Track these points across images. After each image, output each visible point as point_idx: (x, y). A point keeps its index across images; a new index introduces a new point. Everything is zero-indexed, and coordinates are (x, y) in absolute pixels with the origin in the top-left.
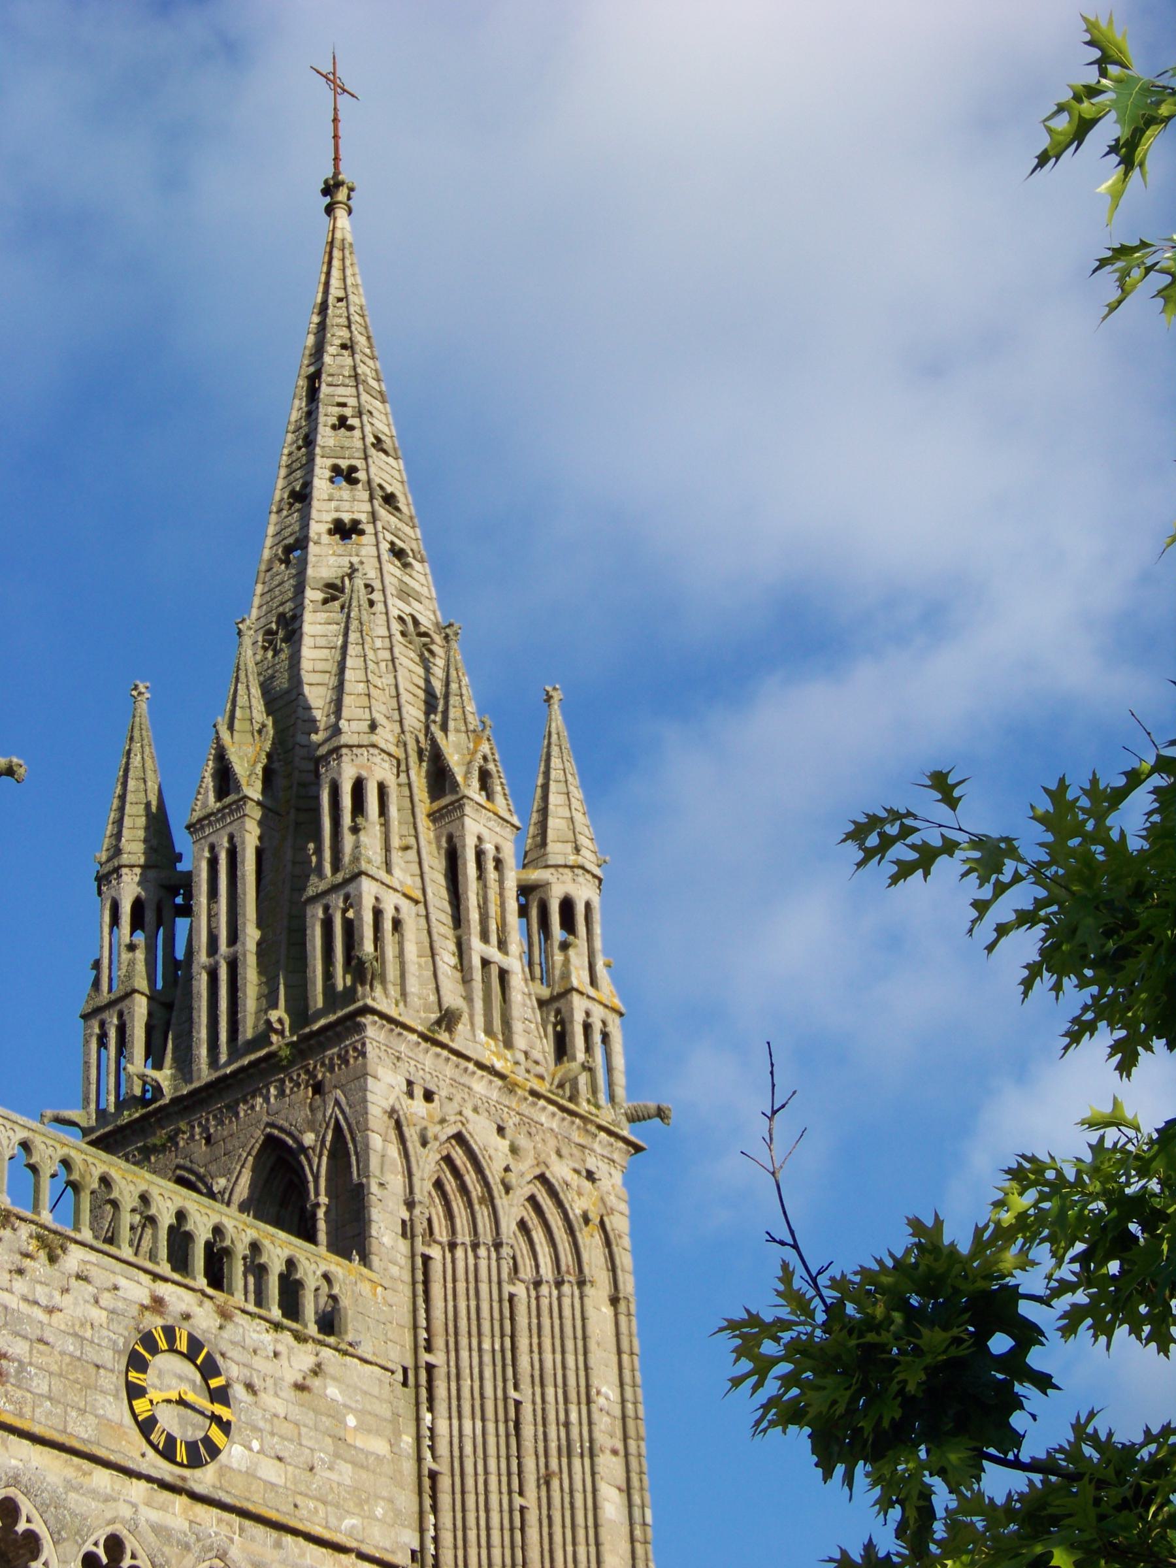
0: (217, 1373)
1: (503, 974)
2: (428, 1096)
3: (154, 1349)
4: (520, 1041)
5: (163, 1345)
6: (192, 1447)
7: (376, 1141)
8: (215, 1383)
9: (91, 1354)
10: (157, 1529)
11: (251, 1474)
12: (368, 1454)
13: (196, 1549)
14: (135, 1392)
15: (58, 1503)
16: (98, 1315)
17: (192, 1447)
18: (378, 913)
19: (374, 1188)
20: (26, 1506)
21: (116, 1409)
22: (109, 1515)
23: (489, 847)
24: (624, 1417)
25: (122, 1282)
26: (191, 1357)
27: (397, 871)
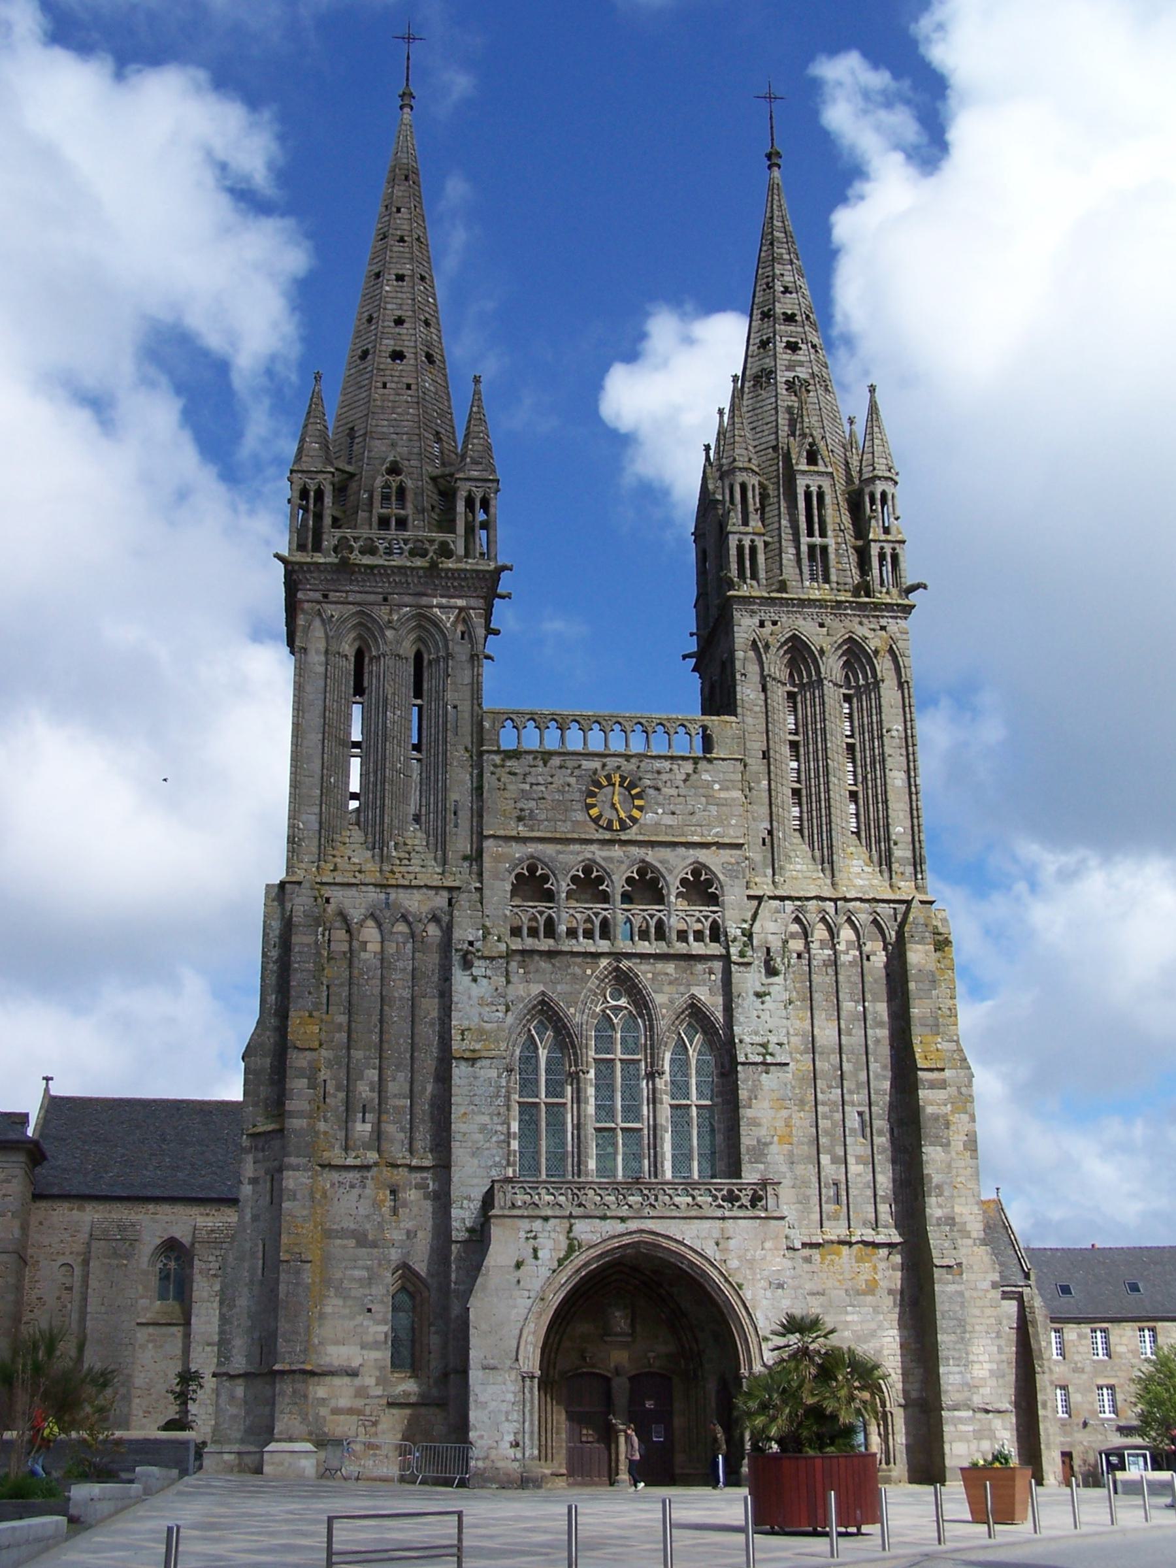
1: (824, 549)
2: (775, 623)
3: (600, 786)
4: (833, 578)
7: (739, 654)
8: (633, 792)
9: (568, 797)
10: (604, 859)
11: (657, 824)
12: (726, 799)
13: (627, 862)
15: (553, 860)
16: (572, 780)
17: (621, 820)
18: (740, 548)
19: (738, 677)
21: (580, 816)
22: (580, 859)
23: (814, 489)
24: (906, 737)
25: (584, 762)
27: (752, 523)
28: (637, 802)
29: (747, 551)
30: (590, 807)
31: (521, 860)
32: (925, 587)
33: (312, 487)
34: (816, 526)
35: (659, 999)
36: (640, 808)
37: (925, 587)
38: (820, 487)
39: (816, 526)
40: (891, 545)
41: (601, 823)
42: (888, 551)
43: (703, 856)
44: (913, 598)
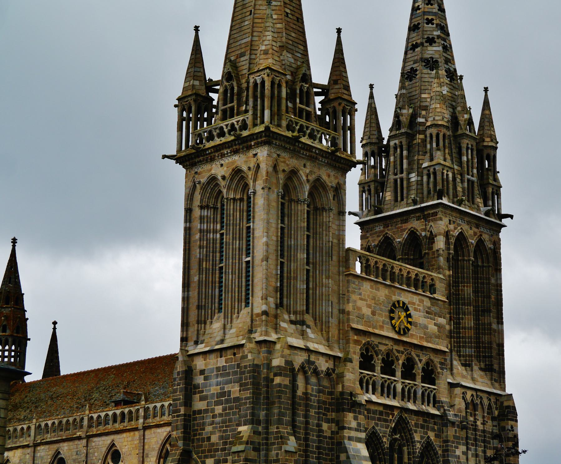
0: (409, 310)
5: (397, 306)
6: (404, 330)
10: (396, 350)
14: (392, 319)
17: (404, 330)
20: (371, 349)
26: (403, 307)
28: (410, 320)
31: (364, 344)
32: (511, 217)
35: (417, 437)
36: (410, 323)
37: (511, 217)
43: (433, 356)
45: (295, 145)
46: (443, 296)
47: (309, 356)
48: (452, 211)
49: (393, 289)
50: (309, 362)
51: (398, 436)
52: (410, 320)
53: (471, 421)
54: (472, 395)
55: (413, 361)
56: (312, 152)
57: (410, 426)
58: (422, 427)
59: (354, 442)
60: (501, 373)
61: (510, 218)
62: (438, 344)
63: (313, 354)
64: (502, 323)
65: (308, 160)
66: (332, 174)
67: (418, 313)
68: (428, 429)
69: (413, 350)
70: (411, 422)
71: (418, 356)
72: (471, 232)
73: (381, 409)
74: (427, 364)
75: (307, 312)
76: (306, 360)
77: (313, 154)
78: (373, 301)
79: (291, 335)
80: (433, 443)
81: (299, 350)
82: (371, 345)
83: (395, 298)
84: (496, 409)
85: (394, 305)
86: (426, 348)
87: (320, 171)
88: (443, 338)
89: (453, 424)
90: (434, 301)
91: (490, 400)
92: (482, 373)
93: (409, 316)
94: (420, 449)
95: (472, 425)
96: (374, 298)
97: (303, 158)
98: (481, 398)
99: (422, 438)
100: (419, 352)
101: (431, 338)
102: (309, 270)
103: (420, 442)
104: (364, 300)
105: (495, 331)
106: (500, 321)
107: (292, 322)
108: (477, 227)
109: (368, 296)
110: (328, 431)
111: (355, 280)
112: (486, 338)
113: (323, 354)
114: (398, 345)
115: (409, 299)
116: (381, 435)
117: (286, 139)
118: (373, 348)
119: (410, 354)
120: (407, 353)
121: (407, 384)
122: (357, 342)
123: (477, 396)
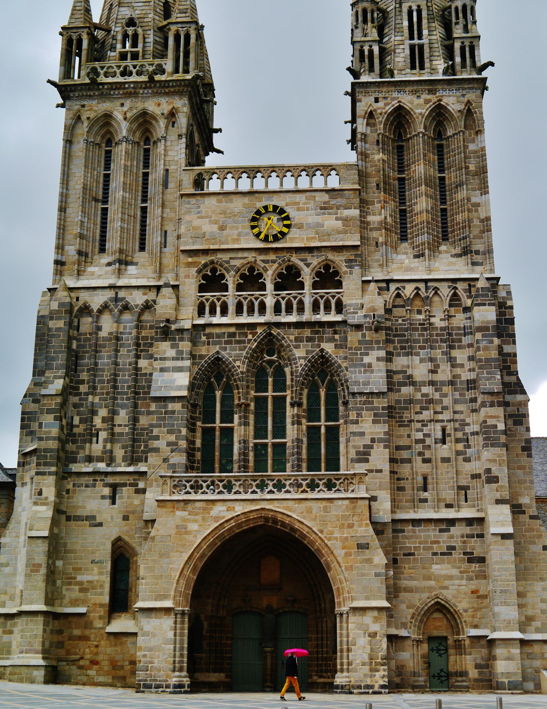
8: (283, 216)
10: (263, 261)
20: (219, 268)
23: (414, 8)
28: (286, 222)
29: (366, 53)
30: (253, 227)
31: (205, 266)
32: (492, 64)
33: (74, 37)
34: (416, 32)
36: (288, 226)
37: (492, 64)
38: (419, 6)
39: (416, 32)
40: (469, 40)
41: (260, 238)
42: (467, 43)
43: (331, 256)
44: (484, 74)
45: (99, 89)
46: (354, 183)
47: (117, 293)
48: (378, 87)
49: (256, 195)
50: (116, 299)
51: (274, 358)
52: (286, 222)
53: (420, 320)
54: (417, 288)
55: (296, 268)
56: (125, 88)
57: (286, 342)
58: (309, 339)
59: (171, 373)
60: (489, 251)
61: (490, 67)
62: (341, 240)
63: (123, 290)
64: (488, 192)
65: (125, 97)
66: (163, 100)
67: (305, 212)
68: (321, 340)
69: (294, 255)
70: (288, 338)
71: (302, 260)
72: (421, 101)
73: (232, 330)
74: (327, 267)
75: (142, 248)
76: (111, 299)
77: (129, 90)
78: (223, 216)
79: (99, 277)
80: (330, 356)
81: (100, 290)
82: (217, 264)
83: (259, 205)
84: (469, 297)
85: (258, 212)
86: (318, 248)
87: (146, 103)
88: (352, 232)
89: (358, 327)
90: (337, 193)
91: (455, 288)
92: (454, 260)
93: (287, 218)
94: (306, 365)
95: (420, 324)
96: (224, 213)
97: (119, 98)
98: (436, 289)
99: (308, 352)
100: (304, 255)
101: (329, 235)
102: (146, 207)
103: (305, 358)
104: (207, 217)
105: (478, 205)
106: (484, 189)
107: (109, 264)
108: (431, 92)
109: (213, 212)
110: (149, 367)
111: (190, 200)
112: (459, 218)
113: (138, 287)
114: (266, 254)
115: (288, 200)
116: (231, 359)
117: (84, 87)
118: (221, 266)
119: (289, 261)
120: (283, 261)
121: (284, 295)
122: (189, 265)
123: (427, 288)
